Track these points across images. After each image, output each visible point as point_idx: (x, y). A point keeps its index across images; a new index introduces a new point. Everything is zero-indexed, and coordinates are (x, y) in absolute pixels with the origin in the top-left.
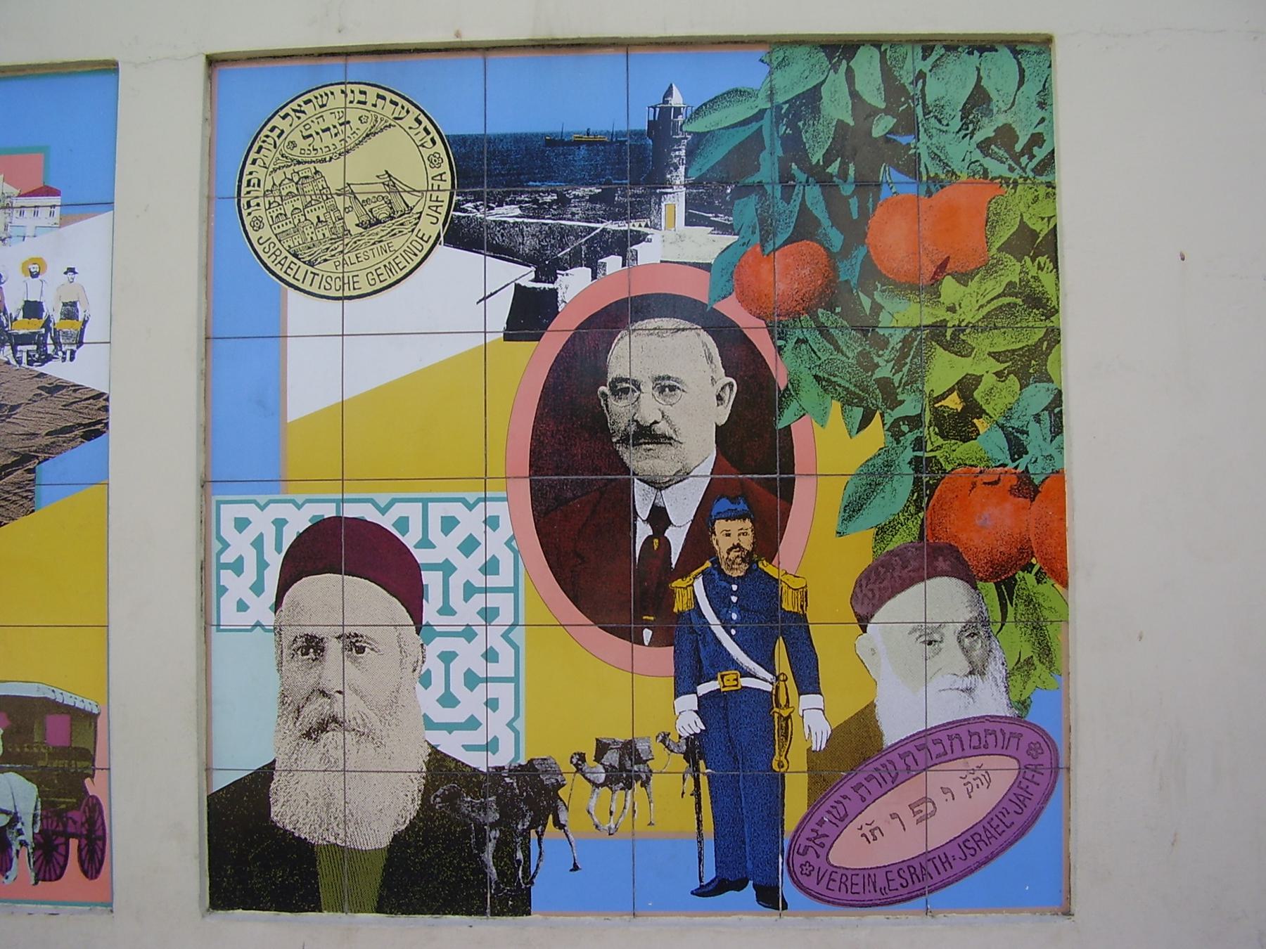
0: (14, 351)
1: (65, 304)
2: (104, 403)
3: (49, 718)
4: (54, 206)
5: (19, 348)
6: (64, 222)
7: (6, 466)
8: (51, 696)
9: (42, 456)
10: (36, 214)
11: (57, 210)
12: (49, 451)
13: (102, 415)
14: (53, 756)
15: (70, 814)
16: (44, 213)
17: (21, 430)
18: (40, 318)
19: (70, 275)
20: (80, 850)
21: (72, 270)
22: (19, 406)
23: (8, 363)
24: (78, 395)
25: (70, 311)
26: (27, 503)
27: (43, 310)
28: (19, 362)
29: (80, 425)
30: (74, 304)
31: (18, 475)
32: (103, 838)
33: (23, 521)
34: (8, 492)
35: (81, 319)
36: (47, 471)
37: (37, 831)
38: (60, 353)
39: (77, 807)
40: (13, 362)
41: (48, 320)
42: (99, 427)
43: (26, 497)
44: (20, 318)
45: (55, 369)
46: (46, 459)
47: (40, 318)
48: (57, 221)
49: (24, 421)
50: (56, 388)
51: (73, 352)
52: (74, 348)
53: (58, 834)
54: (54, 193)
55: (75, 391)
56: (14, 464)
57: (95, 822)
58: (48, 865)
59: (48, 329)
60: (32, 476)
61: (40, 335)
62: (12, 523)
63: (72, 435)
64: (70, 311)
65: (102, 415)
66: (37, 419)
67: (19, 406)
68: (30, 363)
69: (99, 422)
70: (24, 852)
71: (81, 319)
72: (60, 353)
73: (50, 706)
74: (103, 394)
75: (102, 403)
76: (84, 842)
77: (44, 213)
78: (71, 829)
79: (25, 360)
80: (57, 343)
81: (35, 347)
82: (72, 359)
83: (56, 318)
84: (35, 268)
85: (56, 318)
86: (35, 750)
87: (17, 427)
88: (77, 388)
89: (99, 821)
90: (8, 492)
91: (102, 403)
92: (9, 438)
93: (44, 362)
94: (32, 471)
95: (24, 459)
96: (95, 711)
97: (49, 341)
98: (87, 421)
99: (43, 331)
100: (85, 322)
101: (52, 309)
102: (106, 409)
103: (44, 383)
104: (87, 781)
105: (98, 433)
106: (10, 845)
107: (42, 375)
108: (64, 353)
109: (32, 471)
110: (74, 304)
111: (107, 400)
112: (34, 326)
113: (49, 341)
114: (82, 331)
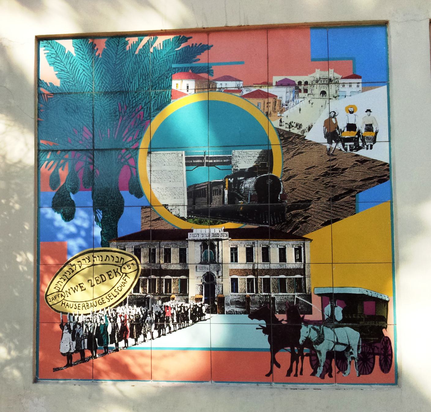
0: (343, 145)
1: (367, 125)
2: (387, 167)
3: (365, 303)
4: (359, 83)
5: (346, 144)
6: (364, 90)
7: (341, 195)
8: (366, 293)
9: (359, 190)
10: (350, 86)
11: (360, 85)
12: (362, 188)
13: (386, 173)
14: (367, 320)
15: (376, 345)
16: (354, 86)
17: (348, 179)
18: (355, 130)
19: (368, 113)
20: (380, 360)
21: (369, 111)
22: (347, 168)
23: (341, 150)
24: (375, 164)
25: (369, 128)
26: (352, 210)
27: (356, 128)
28: (346, 149)
29: (376, 177)
30: (371, 125)
31: (347, 198)
32: (391, 355)
33: (350, 218)
34: (343, 206)
35: (374, 131)
36: (362, 196)
37: (359, 352)
38: (365, 146)
39: (379, 341)
40: (343, 150)
41: (359, 132)
42: (385, 177)
43: (352, 208)
44: (346, 130)
45: (363, 153)
46: (360, 192)
47: (355, 130)
48: (361, 89)
49: (349, 175)
50: (364, 161)
51: (371, 146)
52: (372, 144)
53: (370, 354)
54: (359, 77)
55: (373, 162)
56: (345, 193)
57: (388, 348)
58: (365, 366)
59: (359, 136)
60: (354, 199)
61: (355, 138)
62: (345, 219)
63: (372, 181)
64: (369, 128)
65: (386, 173)
66: (357, 175)
67: (347, 168)
68: (351, 150)
69: (386, 175)
70: (353, 362)
71: (374, 131)
72: (365, 146)
73: (363, 298)
74: (387, 163)
75: (386, 167)
76: (382, 357)
77: (354, 86)
78: (376, 351)
79: (348, 149)
80: (363, 140)
81: (353, 143)
82: (371, 148)
83: (363, 131)
84: (351, 110)
85: (363, 131)
86: (358, 317)
87: (346, 178)
88: (374, 161)
89: (389, 348)
90: (343, 206)
91: (386, 167)
92: (342, 182)
93: (357, 150)
94: (354, 196)
95: (350, 191)
96: (387, 299)
97: (360, 141)
98: (379, 175)
99: (357, 136)
100: (376, 133)
101: (361, 127)
102: (388, 170)
103: (358, 159)
104: (384, 330)
105: (385, 180)
106: (346, 359)
107: (357, 155)
108: (367, 146)
109: (354, 196)
110: (371, 125)
111: (388, 166)
112: (352, 134)
113: (360, 141)
114: (375, 137)
